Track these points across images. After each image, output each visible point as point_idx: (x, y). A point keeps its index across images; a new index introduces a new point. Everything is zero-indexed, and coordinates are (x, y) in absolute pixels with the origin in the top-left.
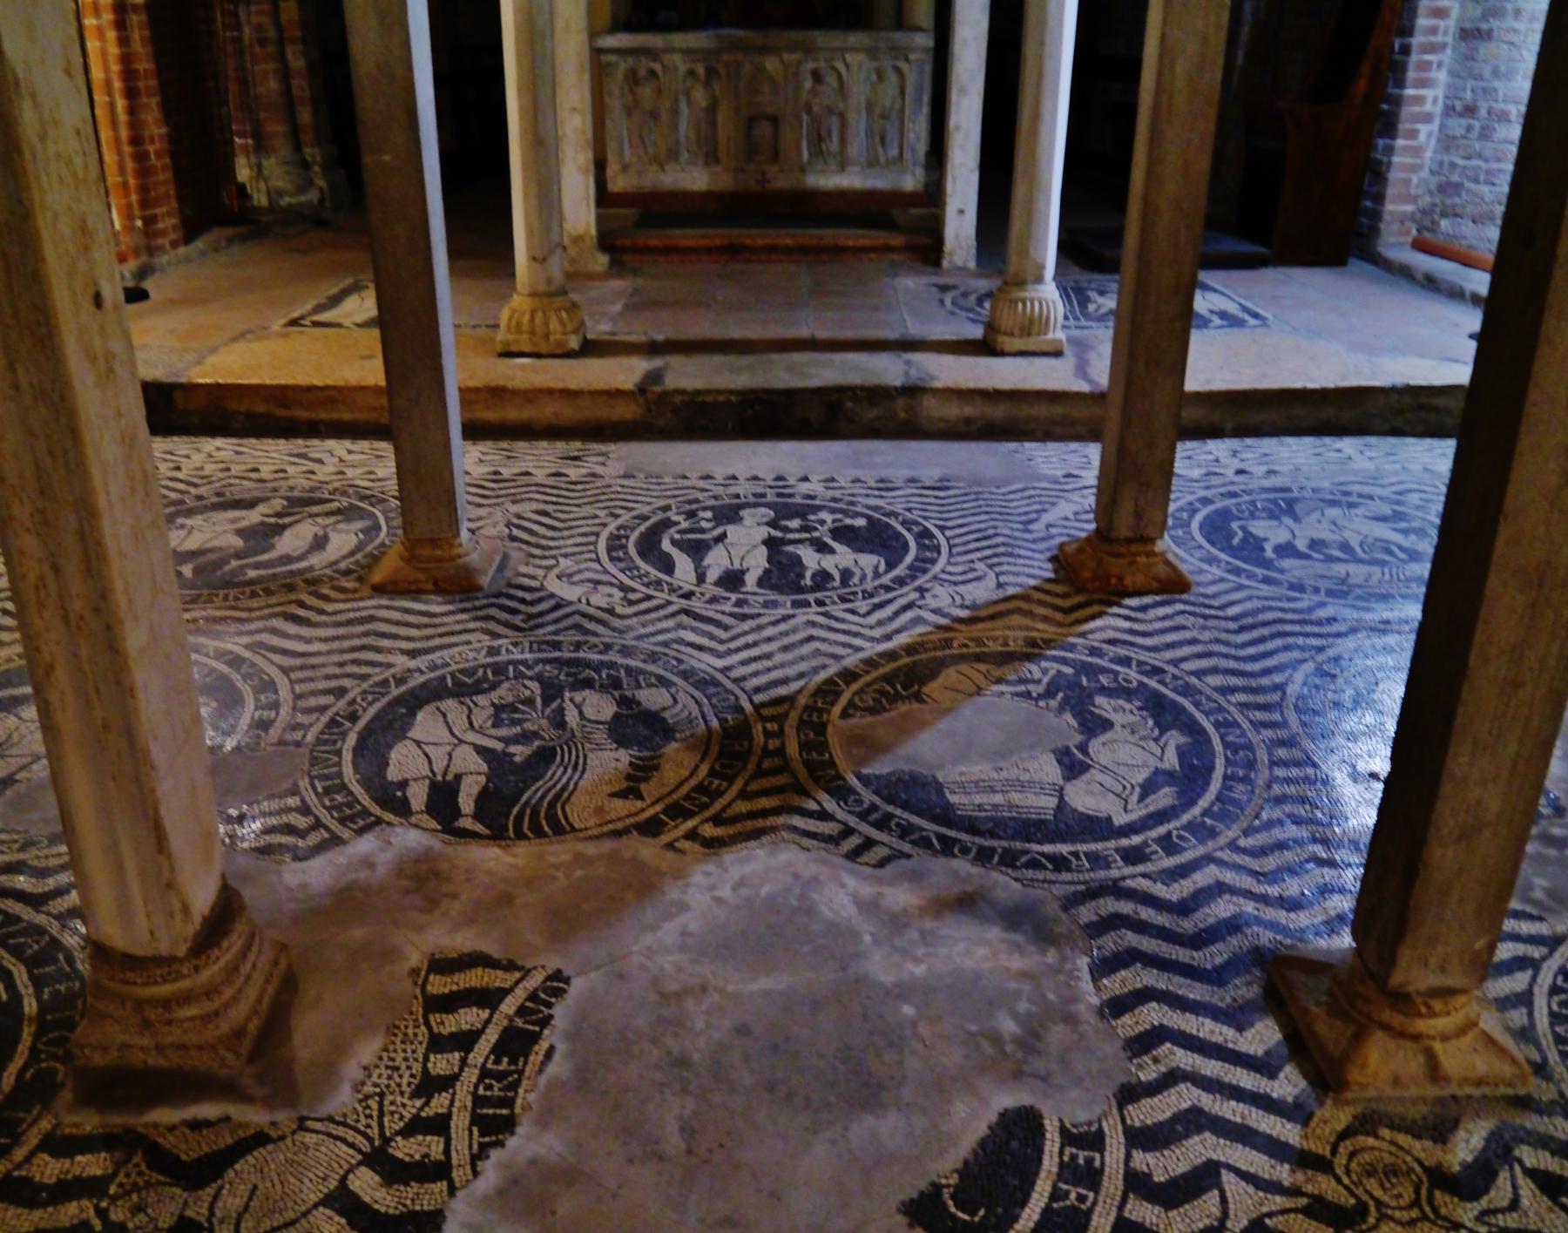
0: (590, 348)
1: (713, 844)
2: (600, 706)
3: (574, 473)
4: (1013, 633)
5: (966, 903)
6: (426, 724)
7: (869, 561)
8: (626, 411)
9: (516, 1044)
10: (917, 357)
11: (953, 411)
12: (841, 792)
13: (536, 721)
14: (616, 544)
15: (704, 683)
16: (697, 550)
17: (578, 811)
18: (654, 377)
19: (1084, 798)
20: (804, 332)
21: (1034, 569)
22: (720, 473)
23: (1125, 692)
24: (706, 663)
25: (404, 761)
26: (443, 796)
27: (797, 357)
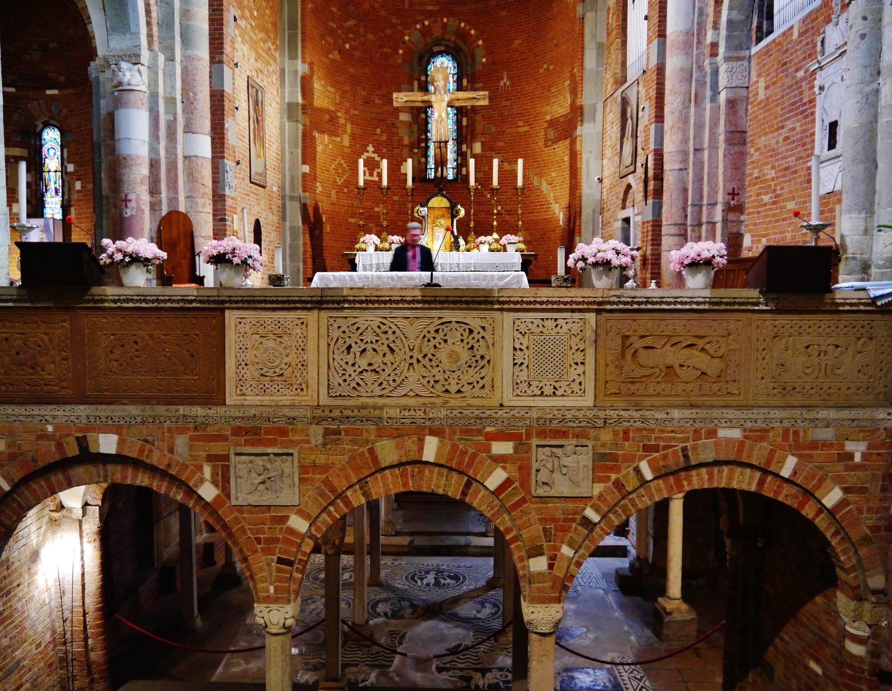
0: (398, 534)
1: (425, 620)
2: (407, 603)
3: (396, 563)
4: (475, 595)
5: (459, 626)
6: (380, 605)
7: (453, 582)
8: (406, 549)
9: (403, 637)
10: (469, 537)
11: (476, 550)
12: (444, 614)
13: (398, 605)
14: (406, 578)
15: (423, 600)
16: (422, 579)
17: (406, 616)
18: (411, 542)
19: (479, 616)
20: (445, 529)
21: (482, 583)
22: (426, 564)
23: (490, 603)
24: (424, 597)
25: (378, 610)
26: (386, 615)
27: (443, 537)
